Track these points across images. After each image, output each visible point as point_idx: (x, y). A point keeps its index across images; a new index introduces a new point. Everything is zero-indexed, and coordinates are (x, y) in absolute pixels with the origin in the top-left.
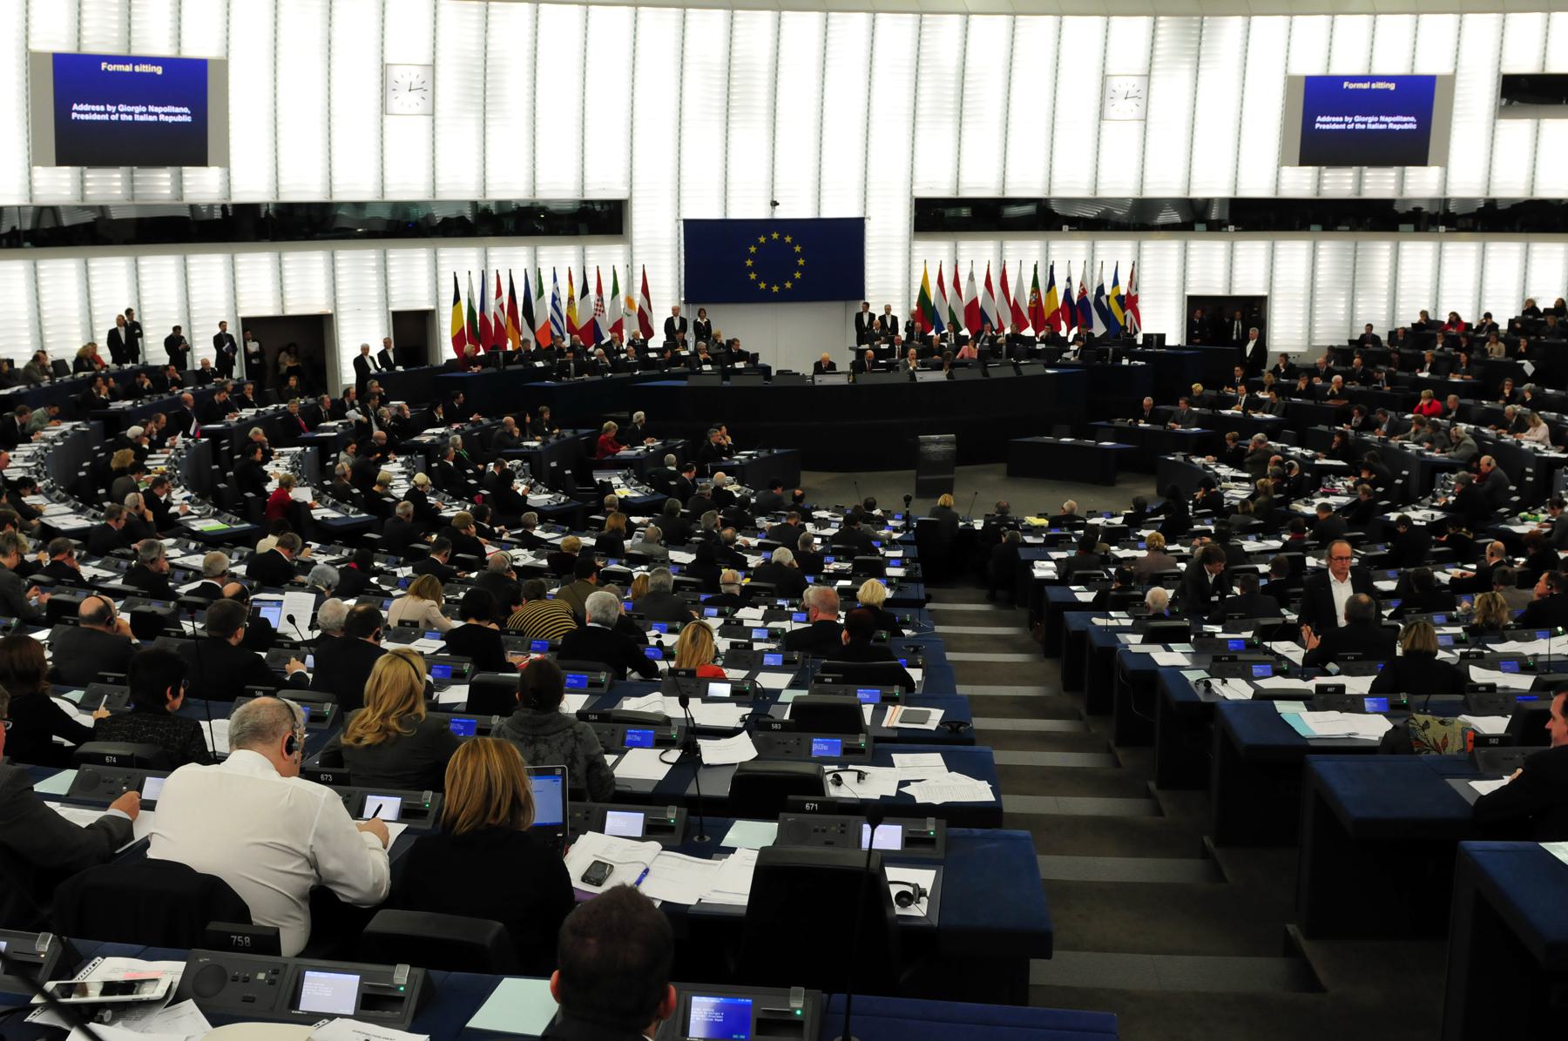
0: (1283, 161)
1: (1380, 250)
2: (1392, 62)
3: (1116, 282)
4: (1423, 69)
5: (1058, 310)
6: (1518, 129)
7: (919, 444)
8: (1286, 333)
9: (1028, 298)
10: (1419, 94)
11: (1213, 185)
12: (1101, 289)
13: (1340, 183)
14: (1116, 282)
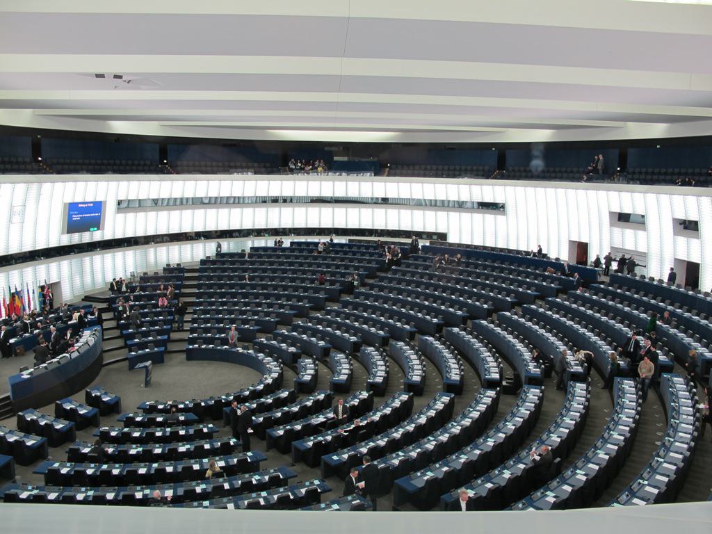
1: (87, 259)
2: (90, 198)
4: (98, 200)
8: (68, 294)
10: (98, 206)
13: (76, 239)
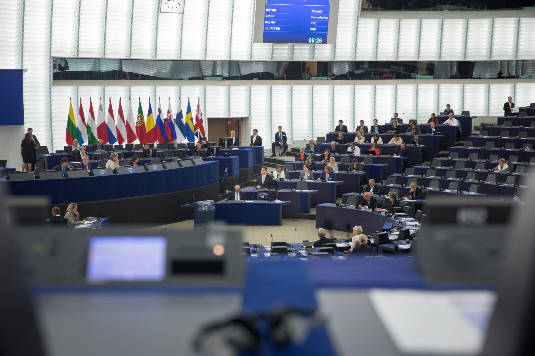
0: (256, 40)
3: (189, 110)
5: (155, 128)
6: (369, 24)
7: (198, 206)
9: (135, 121)
11: (218, 53)
12: (180, 115)
13: (284, 53)
14: (189, 110)
